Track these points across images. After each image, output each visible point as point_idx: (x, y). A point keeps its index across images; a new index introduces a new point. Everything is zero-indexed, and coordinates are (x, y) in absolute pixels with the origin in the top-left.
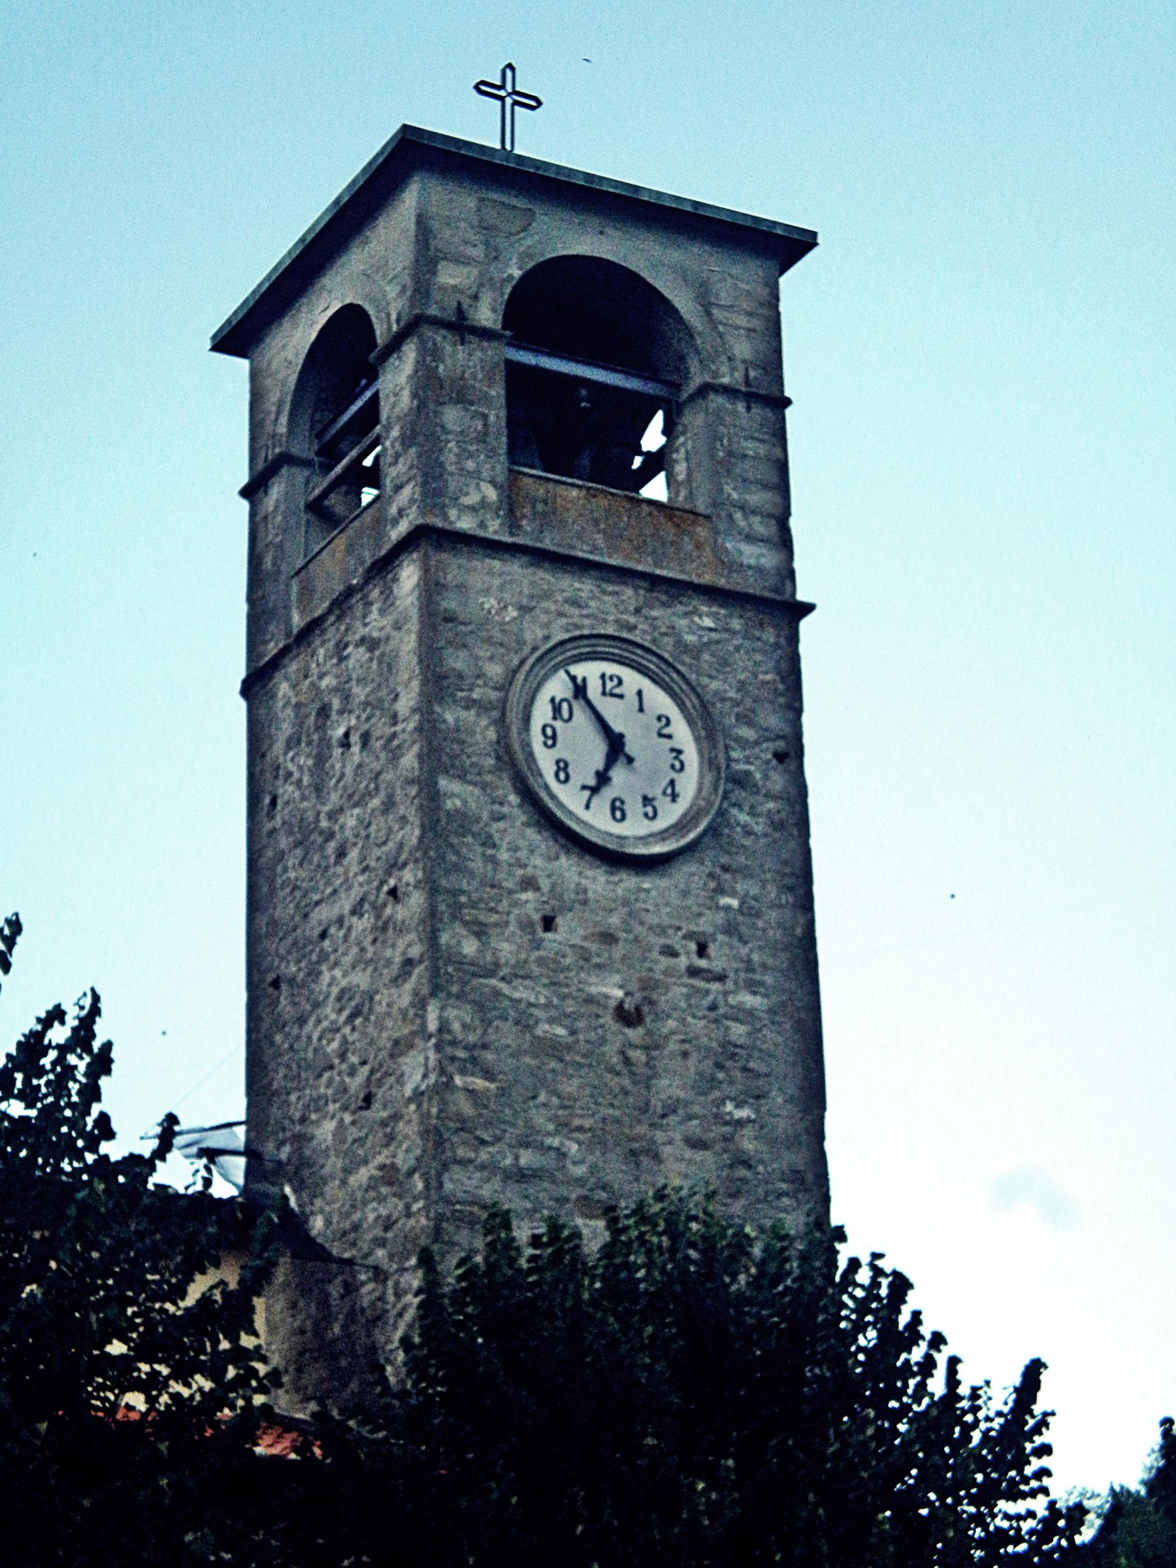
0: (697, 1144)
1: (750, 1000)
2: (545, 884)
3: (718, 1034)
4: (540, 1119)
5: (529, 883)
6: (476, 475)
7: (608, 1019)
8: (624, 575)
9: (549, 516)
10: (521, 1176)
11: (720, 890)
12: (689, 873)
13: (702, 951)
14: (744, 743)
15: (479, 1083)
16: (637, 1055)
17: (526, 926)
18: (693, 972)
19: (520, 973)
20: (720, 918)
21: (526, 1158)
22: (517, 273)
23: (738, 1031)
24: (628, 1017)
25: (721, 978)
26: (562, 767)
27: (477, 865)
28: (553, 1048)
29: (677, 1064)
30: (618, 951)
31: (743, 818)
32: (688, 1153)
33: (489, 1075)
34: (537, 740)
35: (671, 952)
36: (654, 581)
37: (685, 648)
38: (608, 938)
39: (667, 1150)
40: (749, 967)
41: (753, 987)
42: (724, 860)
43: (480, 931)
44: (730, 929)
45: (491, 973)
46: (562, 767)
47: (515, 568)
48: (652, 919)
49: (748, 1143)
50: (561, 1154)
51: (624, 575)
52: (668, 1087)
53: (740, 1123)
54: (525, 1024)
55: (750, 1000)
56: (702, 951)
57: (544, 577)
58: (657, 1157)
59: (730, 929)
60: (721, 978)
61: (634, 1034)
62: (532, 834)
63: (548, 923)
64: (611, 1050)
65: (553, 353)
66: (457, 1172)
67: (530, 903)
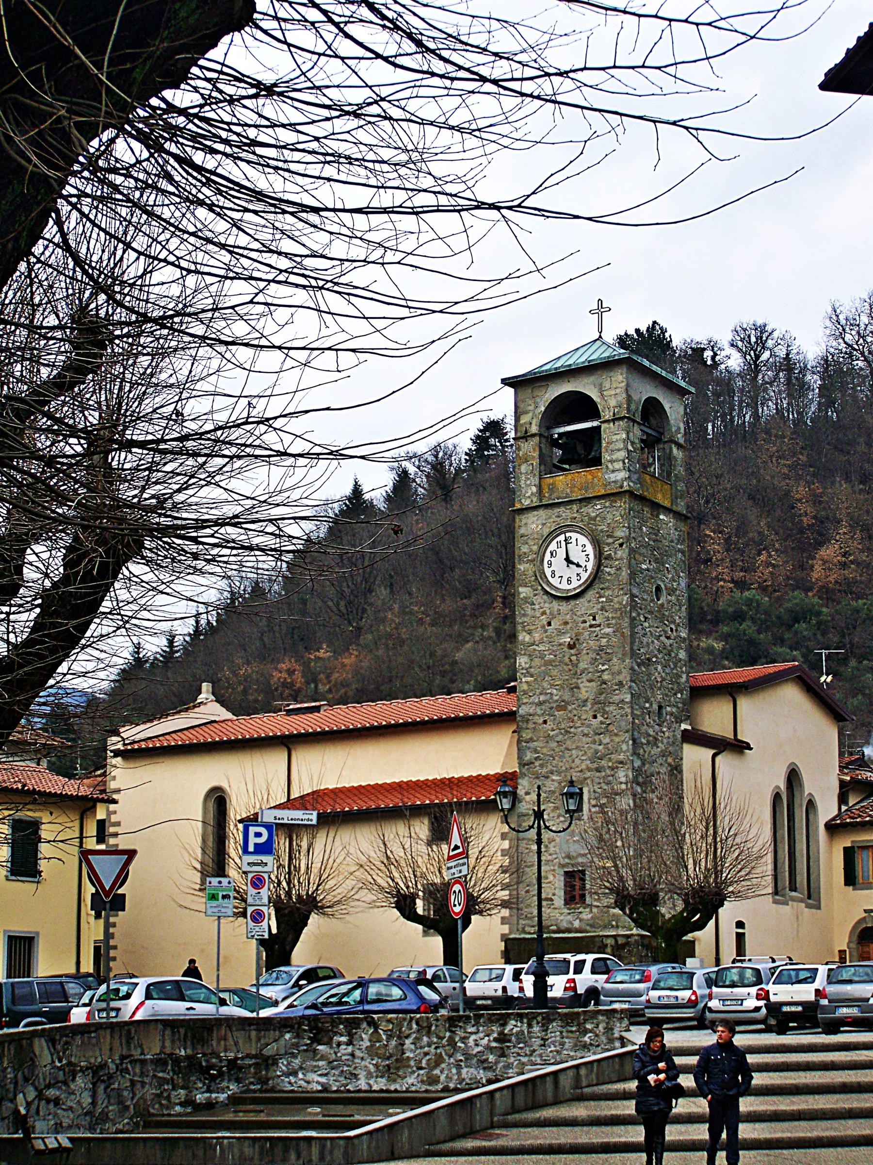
0: (590, 681)
1: (608, 630)
2: (548, 612)
3: (598, 643)
4: (545, 685)
5: (544, 613)
6: (530, 485)
7: (566, 649)
8: (571, 502)
9: (552, 488)
10: (541, 703)
11: (600, 597)
12: (591, 594)
13: (594, 619)
14: (608, 544)
15: (529, 679)
16: (574, 658)
17: (543, 627)
18: (591, 626)
19: (541, 642)
20: (599, 606)
21: (542, 698)
22: (543, 409)
23: (604, 641)
24: (571, 647)
25: (599, 625)
26: (553, 572)
27: (529, 612)
28: (550, 662)
29: (586, 657)
30: (568, 627)
31: (608, 570)
32: (588, 684)
33: (532, 676)
34: (546, 565)
35: (585, 622)
36: (580, 500)
37: (591, 519)
38: (566, 623)
39: (581, 685)
40: (608, 619)
41: (608, 626)
42: (602, 586)
43: (530, 632)
44: (602, 609)
45: (533, 644)
46: (553, 572)
47: (541, 512)
48: (579, 613)
49: (606, 677)
50: (551, 694)
51: (571, 502)
52: (582, 665)
53: (603, 671)
54: (542, 657)
55: (608, 630)
56: (594, 619)
57: (549, 512)
58: (578, 688)
59: (602, 609)
60: (599, 625)
61: (572, 651)
62: (545, 597)
63: (549, 624)
64: (566, 659)
65: (569, 423)
66: (523, 707)
67: (544, 620)
